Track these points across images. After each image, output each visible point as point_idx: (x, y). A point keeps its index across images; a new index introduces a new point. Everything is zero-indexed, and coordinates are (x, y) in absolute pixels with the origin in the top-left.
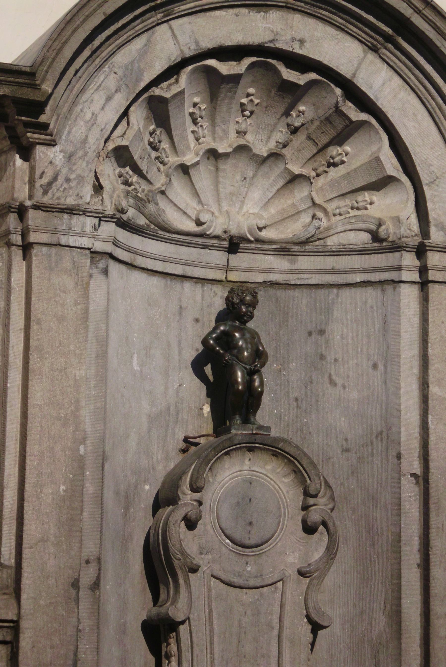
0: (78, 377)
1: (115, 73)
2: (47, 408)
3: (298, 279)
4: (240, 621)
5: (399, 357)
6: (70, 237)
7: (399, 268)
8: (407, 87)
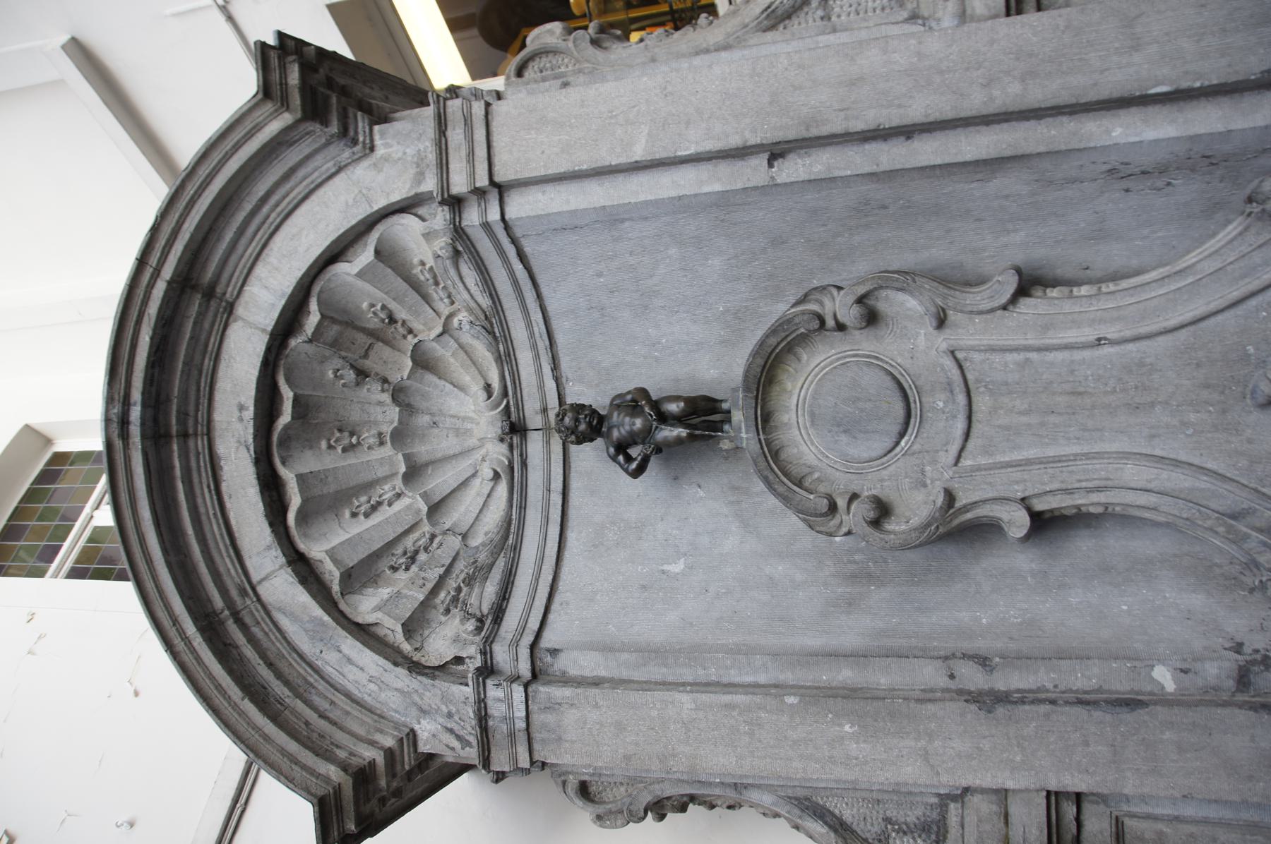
0: (693, 706)
4: (1020, 413)
7: (486, 226)
8: (264, 255)
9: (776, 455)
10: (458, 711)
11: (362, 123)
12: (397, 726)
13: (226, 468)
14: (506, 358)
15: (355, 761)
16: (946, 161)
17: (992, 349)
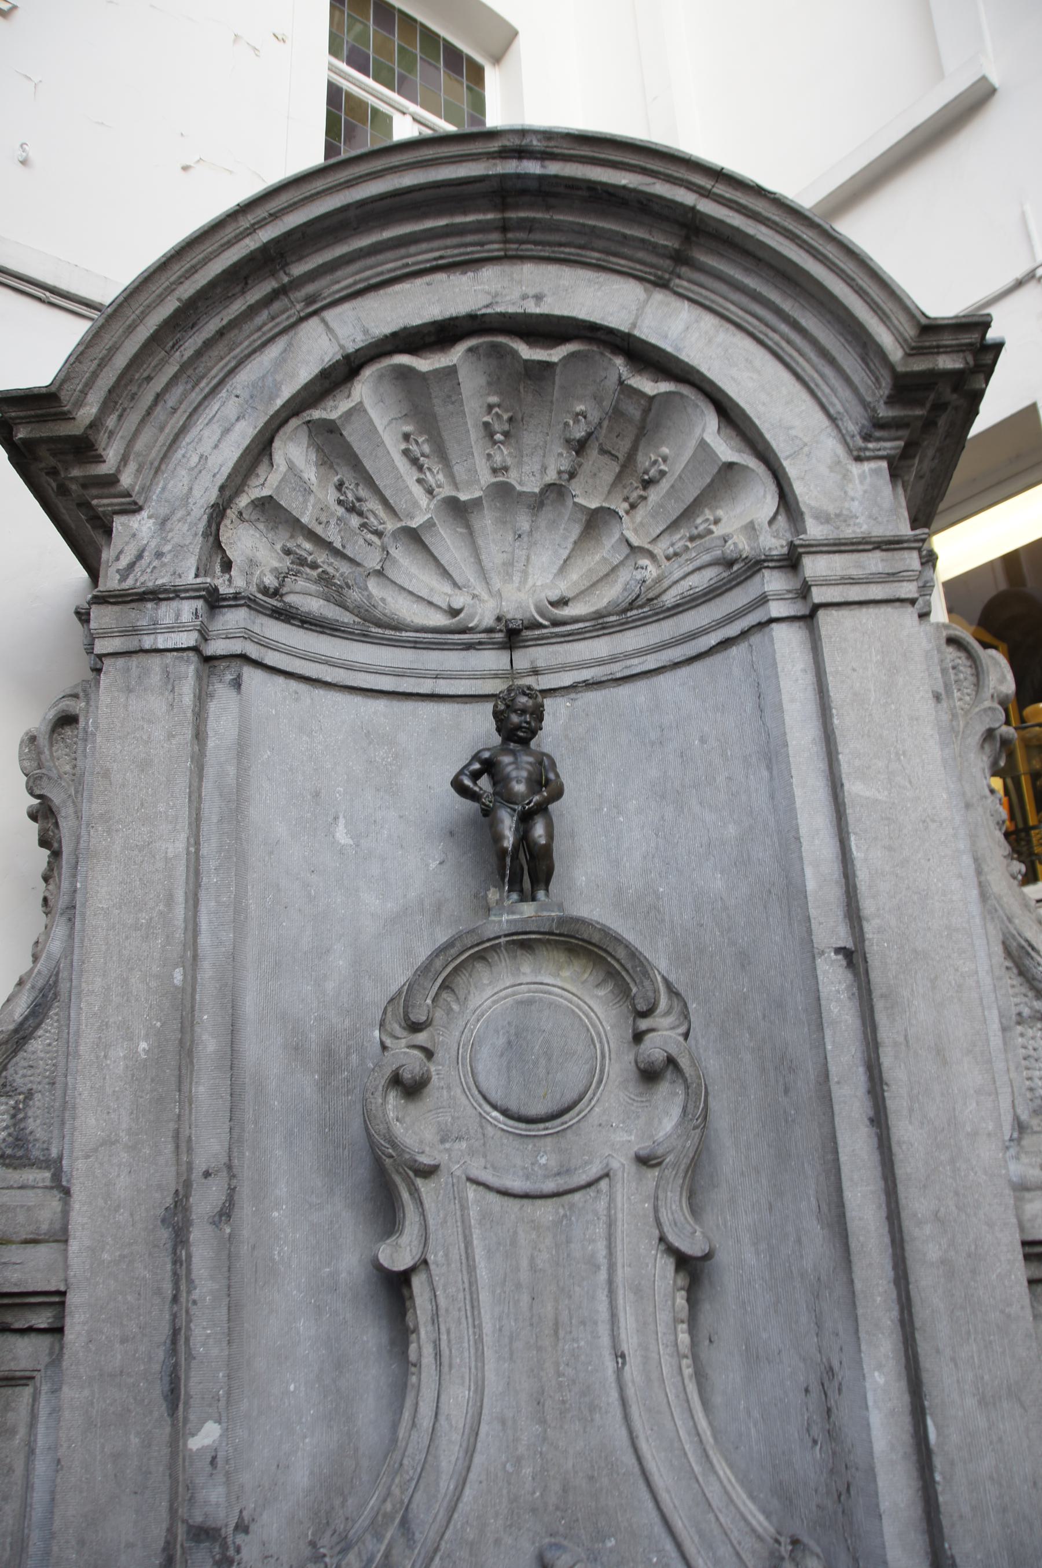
0: (170, 855)
1: (237, 396)
2: (117, 911)
3: (626, 667)
4: (532, 1259)
5: (786, 745)
6: (159, 636)
7: (763, 600)
9: (481, 957)
10: (164, 565)
11: (890, 447)
12: (146, 489)
13: (464, 279)
14: (600, 624)
15: (102, 438)
16: (842, 1167)
17: (611, 1224)
